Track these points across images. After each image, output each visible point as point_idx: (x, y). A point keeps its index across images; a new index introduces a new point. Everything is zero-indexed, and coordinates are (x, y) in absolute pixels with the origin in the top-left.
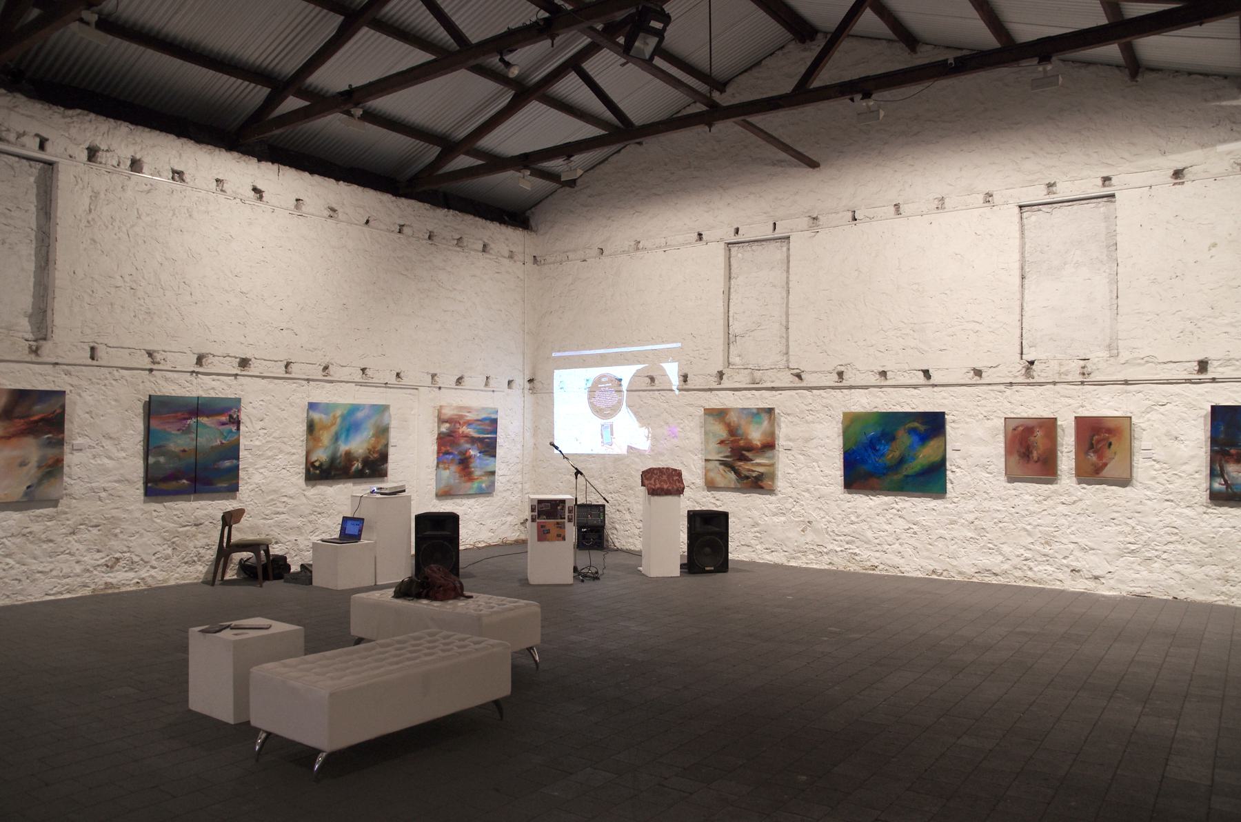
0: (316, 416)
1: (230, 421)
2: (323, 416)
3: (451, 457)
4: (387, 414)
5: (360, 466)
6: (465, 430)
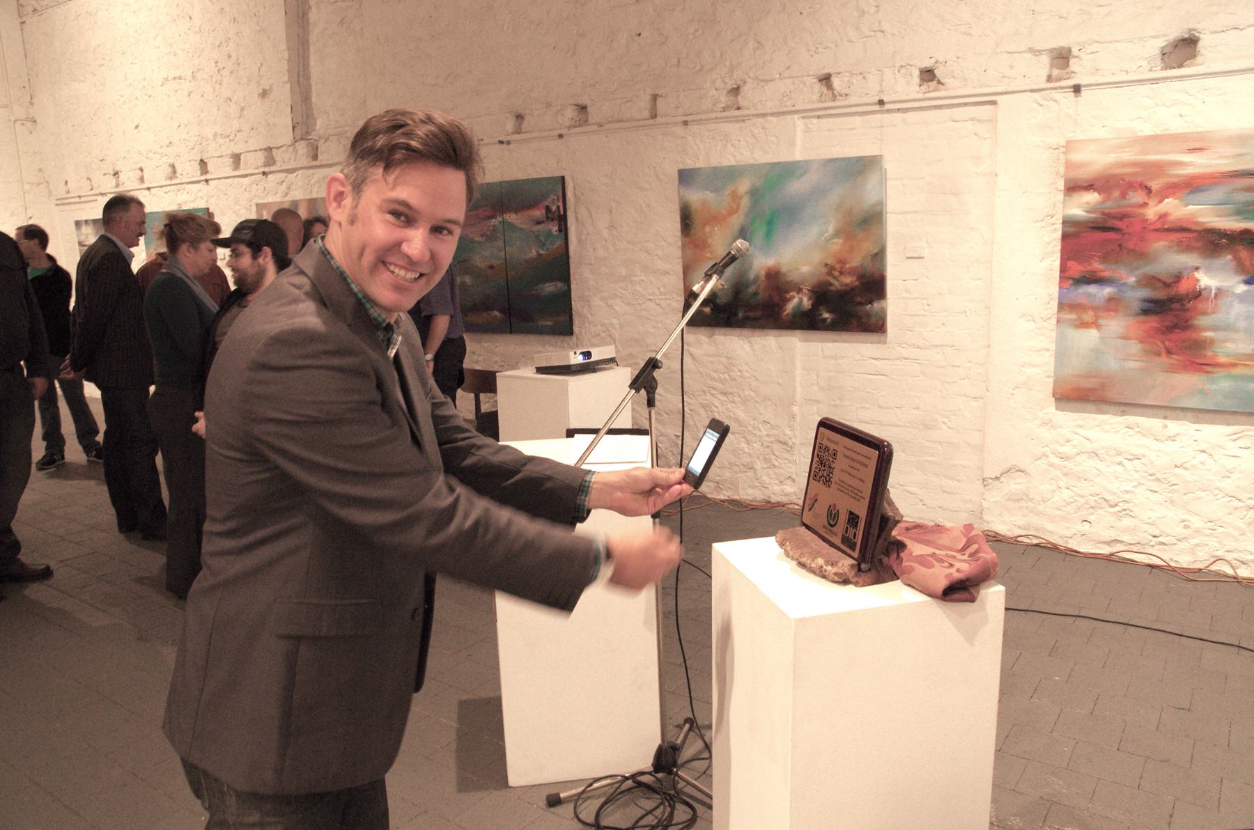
0: (695, 197)
1: (547, 217)
2: (709, 196)
3: (1107, 291)
4: (872, 181)
5: (807, 303)
6: (1176, 208)
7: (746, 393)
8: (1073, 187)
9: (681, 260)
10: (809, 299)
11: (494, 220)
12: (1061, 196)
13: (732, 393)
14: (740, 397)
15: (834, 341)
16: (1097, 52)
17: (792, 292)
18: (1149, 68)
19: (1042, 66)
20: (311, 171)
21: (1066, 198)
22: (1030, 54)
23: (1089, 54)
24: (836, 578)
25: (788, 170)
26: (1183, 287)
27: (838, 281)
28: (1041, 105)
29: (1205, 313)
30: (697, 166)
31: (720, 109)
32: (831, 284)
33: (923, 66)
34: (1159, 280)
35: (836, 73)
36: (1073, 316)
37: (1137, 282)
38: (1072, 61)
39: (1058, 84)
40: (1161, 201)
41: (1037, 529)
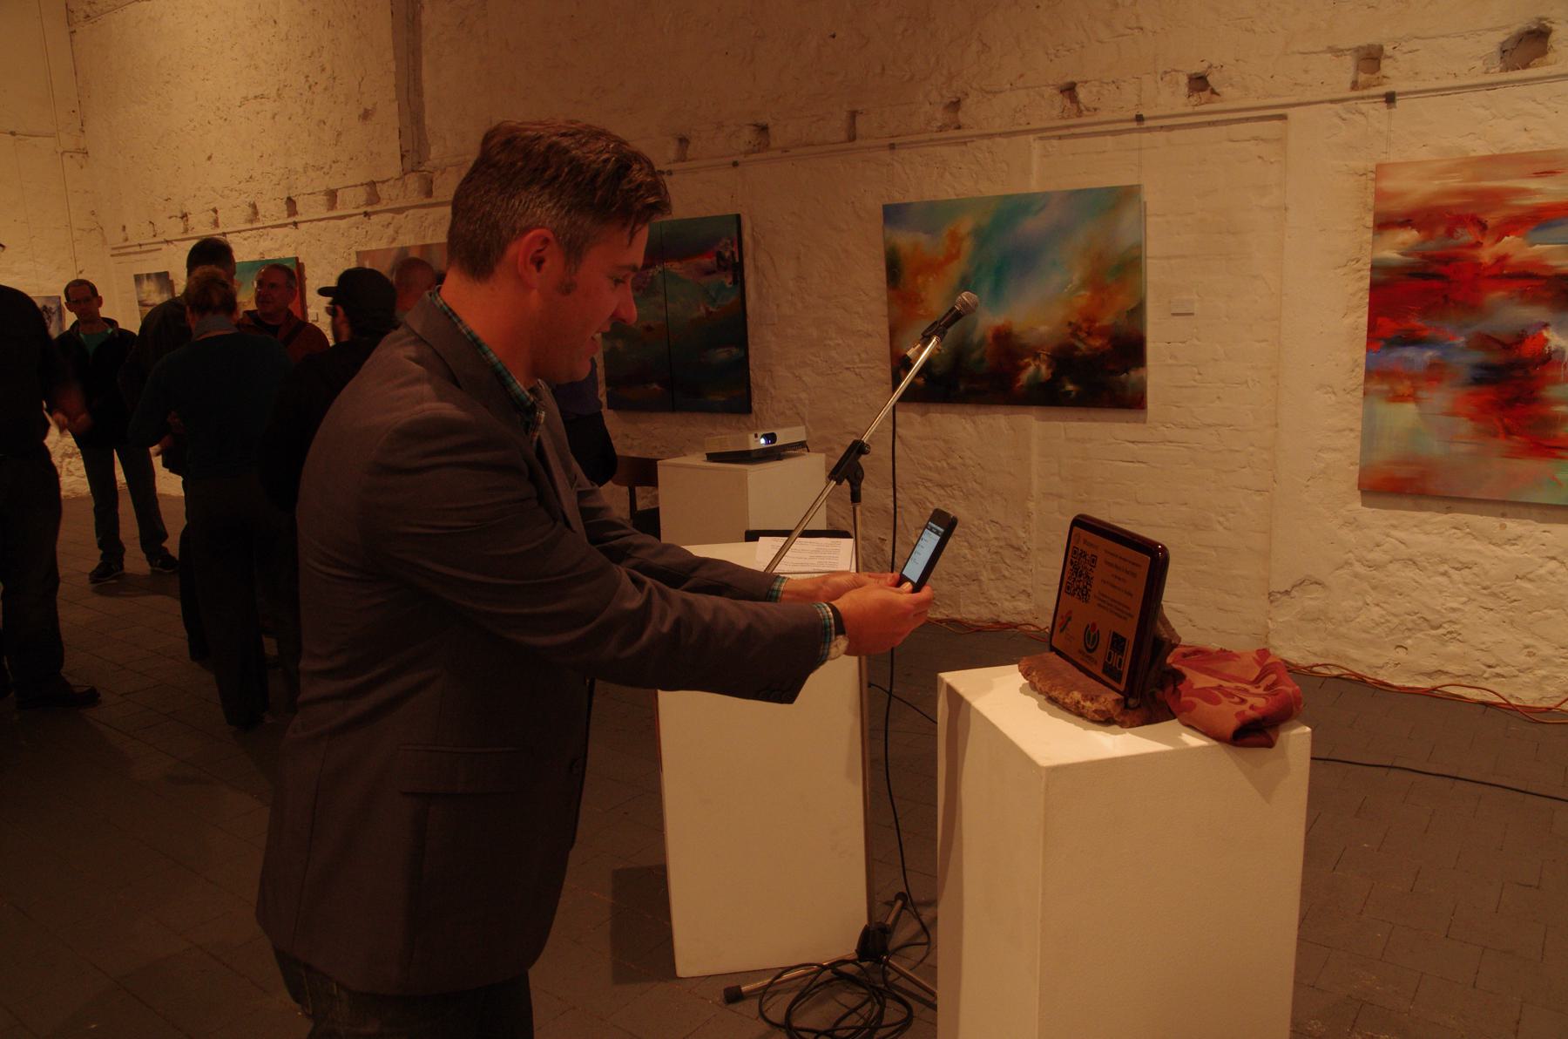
0: (905, 240)
1: (719, 266)
2: (923, 238)
3: (1429, 354)
6: (1516, 247)
7: (970, 485)
8: (1385, 224)
9: (886, 319)
10: (1048, 368)
11: (651, 271)
12: (1369, 235)
13: (951, 486)
14: (962, 491)
15: (1080, 420)
16: (1417, 50)
17: (1025, 358)
18: (1484, 69)
19: (1345, 70)
20: (424, 211)
21: (1376, 237)
22: (1329, 55)
23: (1405, 53)
24: (1096, 716)
25: (1017, 207)
26: (1527, 350)
27: (1085, 344)
28: (1344, 120)
29: (1555, 381)
30: (907, 201)
31: (935, 129)
32: (1076, 348)
33: (1194, 72)
34: (1497, 341)
35: (1082, 82)
36: (1385, 387)
37: (1467, 343)
38: (1384, 63)
39: (1366, 93)
40: (1499, 240)
41: (1338, 657)
